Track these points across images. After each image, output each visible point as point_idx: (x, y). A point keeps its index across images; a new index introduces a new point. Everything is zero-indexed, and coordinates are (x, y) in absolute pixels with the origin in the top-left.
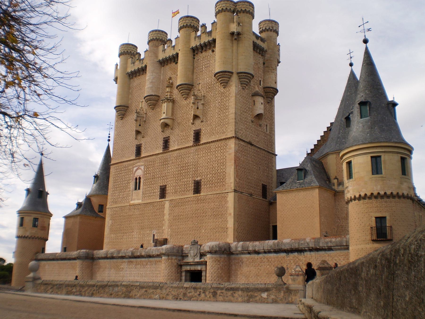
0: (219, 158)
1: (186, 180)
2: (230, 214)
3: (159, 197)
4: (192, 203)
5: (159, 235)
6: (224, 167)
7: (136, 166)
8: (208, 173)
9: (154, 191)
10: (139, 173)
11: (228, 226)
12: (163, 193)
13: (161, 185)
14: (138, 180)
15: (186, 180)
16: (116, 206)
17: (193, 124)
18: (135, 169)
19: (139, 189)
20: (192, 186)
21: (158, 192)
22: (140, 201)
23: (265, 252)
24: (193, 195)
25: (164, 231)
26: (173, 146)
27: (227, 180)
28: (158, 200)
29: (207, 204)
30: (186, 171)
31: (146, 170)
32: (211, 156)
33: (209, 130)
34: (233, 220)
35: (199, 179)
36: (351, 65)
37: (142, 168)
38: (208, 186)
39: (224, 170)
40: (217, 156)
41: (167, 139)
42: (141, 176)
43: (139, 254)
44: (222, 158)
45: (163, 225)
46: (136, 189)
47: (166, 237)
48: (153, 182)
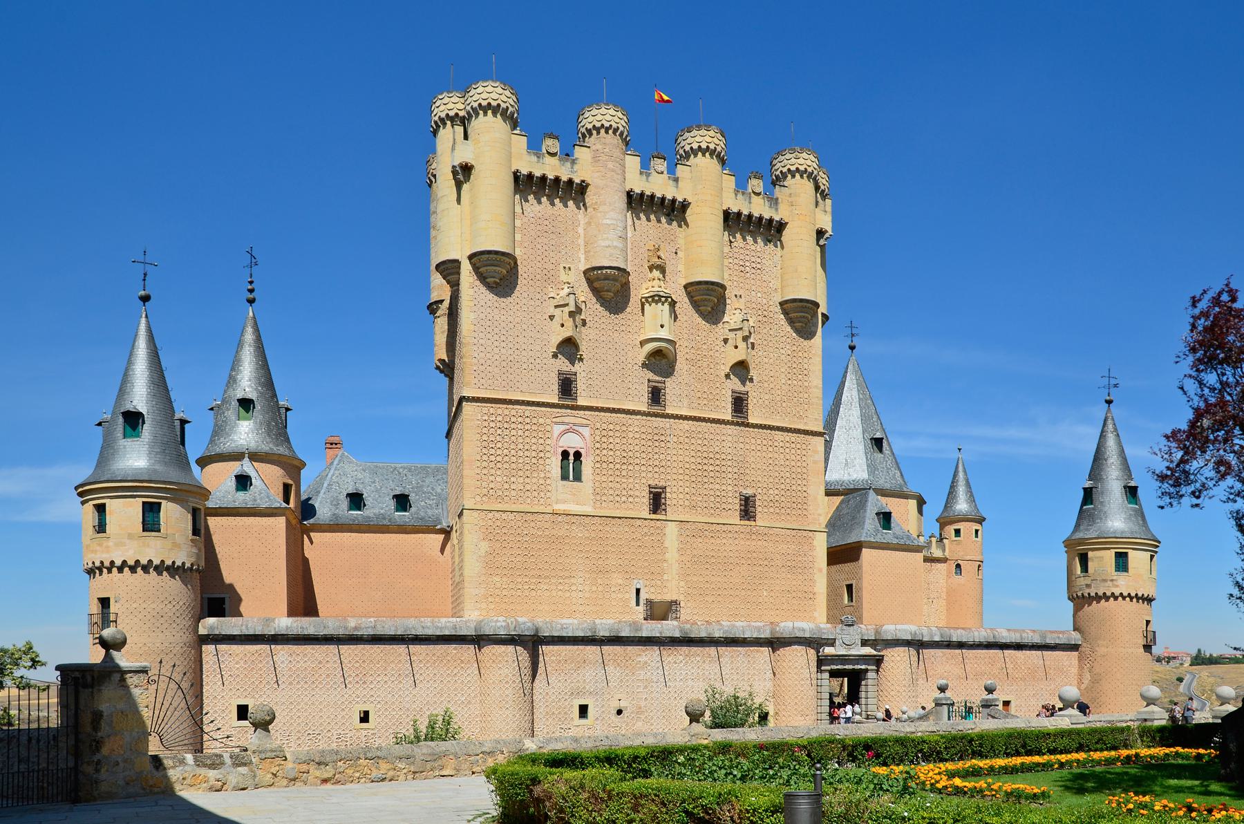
1: (717, 486)
7: (563, 423)
9: (631, 493)
10: (572, 442)
12: (657, 501)
14: (571, 458)
15: (717, 486)
16: (500, 507)
18: (558, 429)
19: (578, 478)
21: (645, 500)
22: (588, 510)
28: (646, 514)
30: (717, 468)
31: (598, 438)
35: (749, 492)
42: (582, 451)
46: (565, 477)
48: (624, 473)
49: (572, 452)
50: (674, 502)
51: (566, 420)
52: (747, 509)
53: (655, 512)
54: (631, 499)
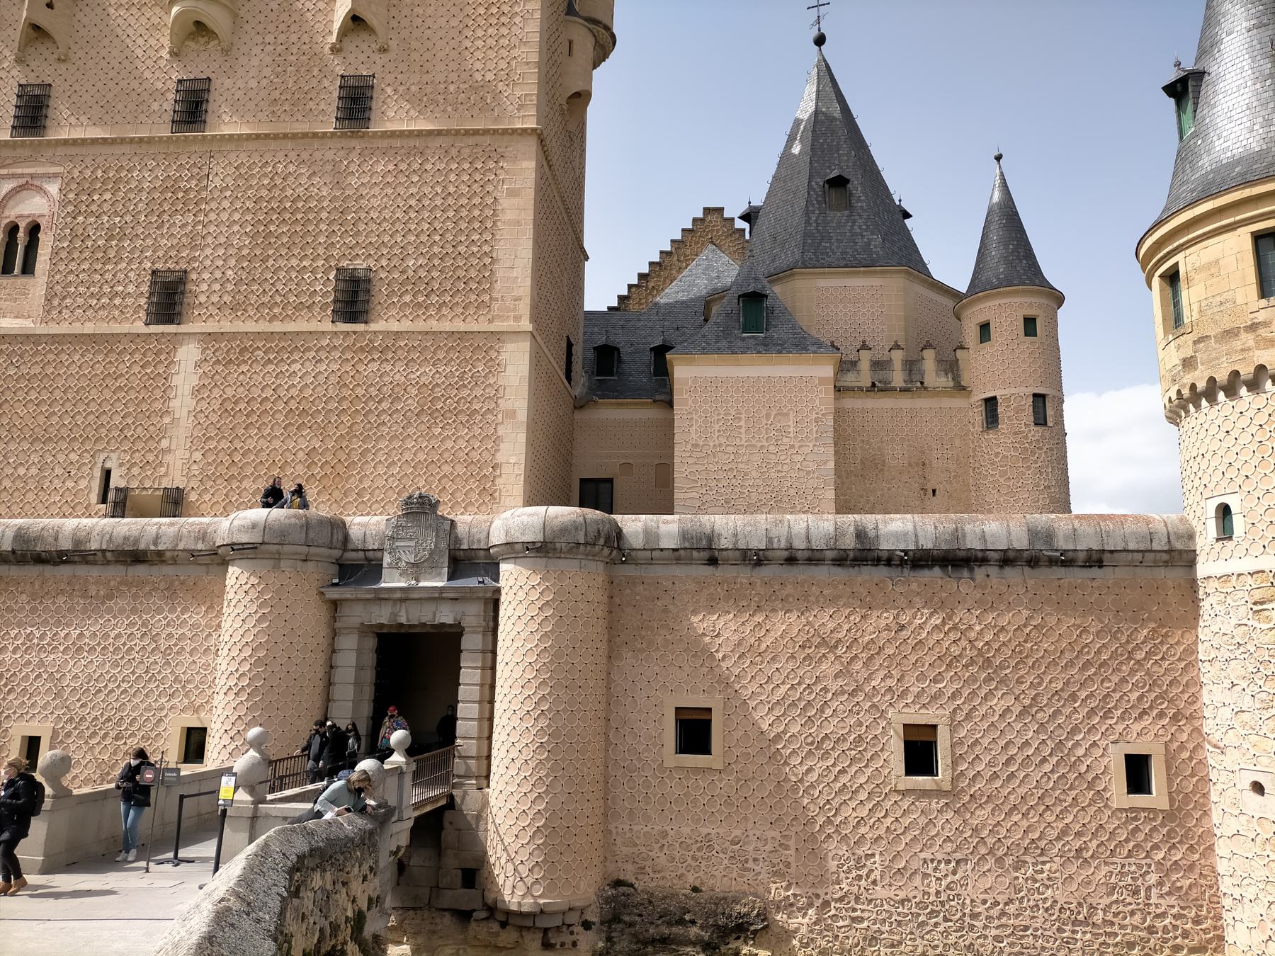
0: (464, 201)
1: (294, 262)
2: (512, 414)
3: (142, 314)
4: (323, 355)
5: (135, 471)
6: (487, 236)
7: (14, 176)
8: (411, 250)
11: (500, 458)
12: (169, 299)
13: (159, 266)
14: (22, 236)
15: (294, 262)
17: (335, 50)
19: (28, 269)
20: (325, 289)
23: (791, 560)
24: (327, 326)
25: (168, 458)
26: (226, 122)
27: (498, 286)
28: (139, 327)
29: (400, 366)
31: (71, 196)
32: (427, 190)
33: (413, 88)
34: (522, 437)
35: (360, 264)
36: (820, 41)
37: (53, 189)
38: (407, 298)
39: (486, 248)
40: (452, 190)
41: (197, 87)
42: (43, 223)
43: (66, 545)
44: (477, 200)
45: (162, 433)
47: (179, 482)
48: (112, 254)
49: (22, 225)
50: (203, 299)
51: (19, 171)
52: (353, 299)
53: (158, 322)
54: (117, 301)
